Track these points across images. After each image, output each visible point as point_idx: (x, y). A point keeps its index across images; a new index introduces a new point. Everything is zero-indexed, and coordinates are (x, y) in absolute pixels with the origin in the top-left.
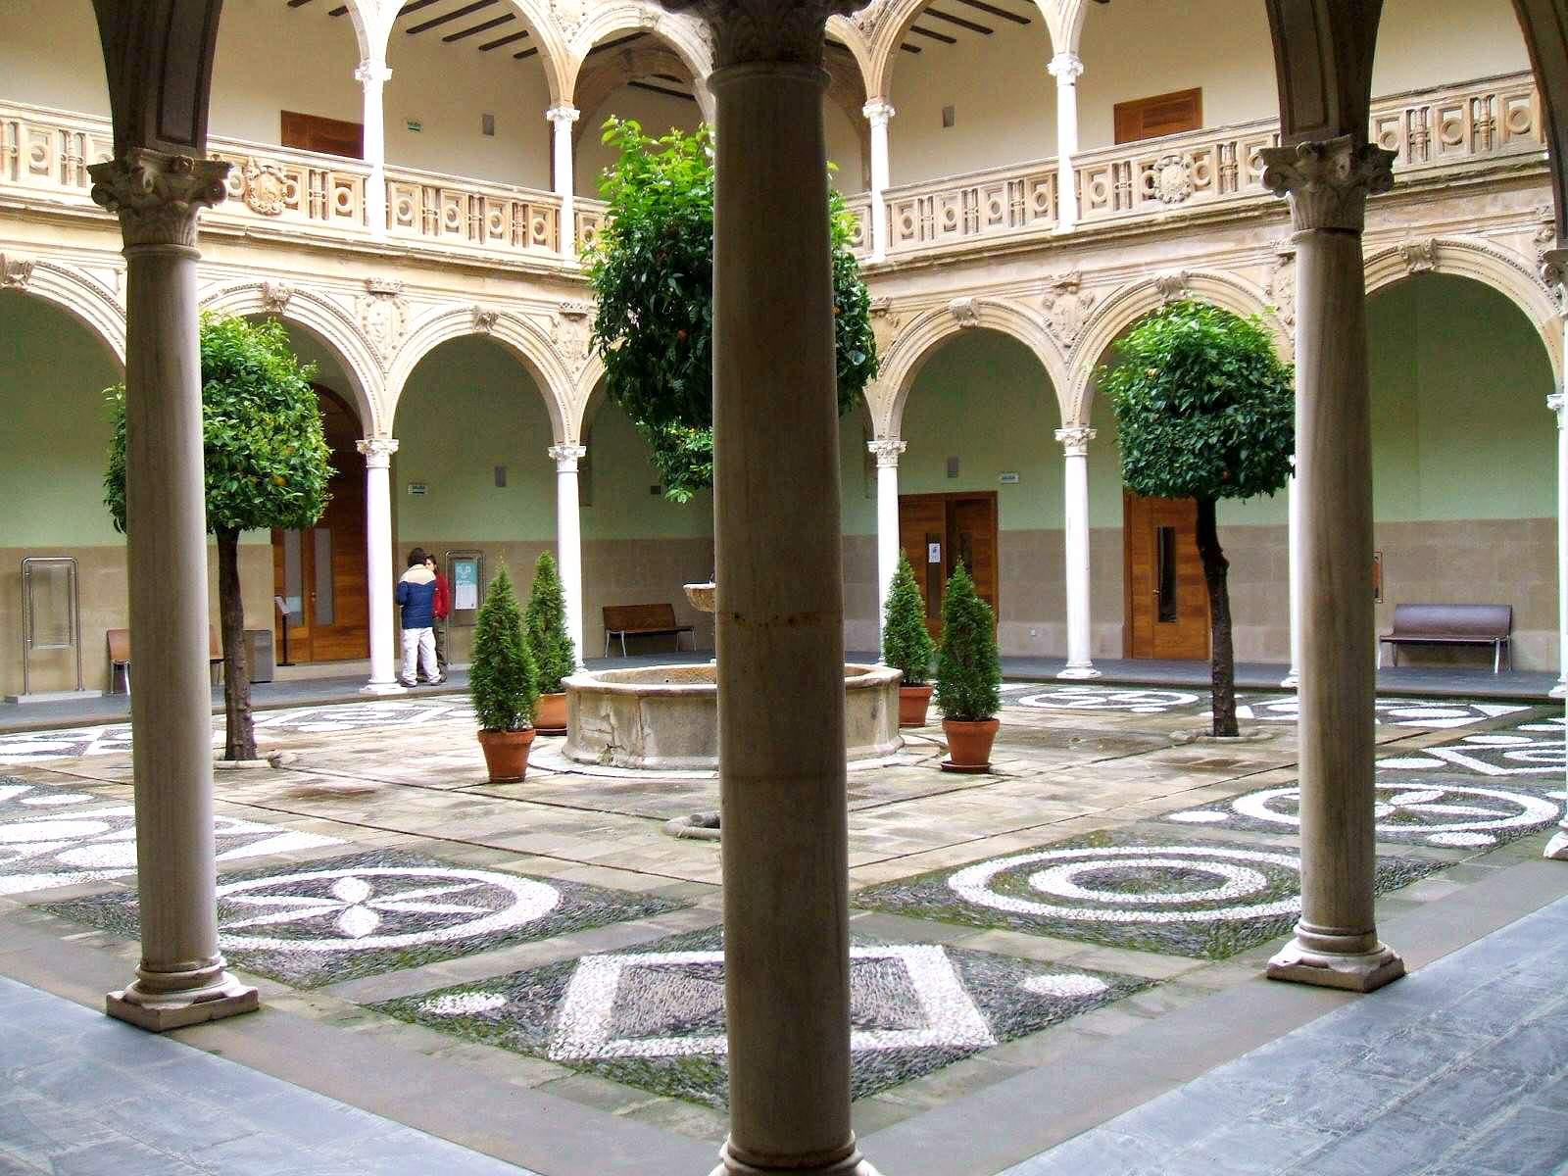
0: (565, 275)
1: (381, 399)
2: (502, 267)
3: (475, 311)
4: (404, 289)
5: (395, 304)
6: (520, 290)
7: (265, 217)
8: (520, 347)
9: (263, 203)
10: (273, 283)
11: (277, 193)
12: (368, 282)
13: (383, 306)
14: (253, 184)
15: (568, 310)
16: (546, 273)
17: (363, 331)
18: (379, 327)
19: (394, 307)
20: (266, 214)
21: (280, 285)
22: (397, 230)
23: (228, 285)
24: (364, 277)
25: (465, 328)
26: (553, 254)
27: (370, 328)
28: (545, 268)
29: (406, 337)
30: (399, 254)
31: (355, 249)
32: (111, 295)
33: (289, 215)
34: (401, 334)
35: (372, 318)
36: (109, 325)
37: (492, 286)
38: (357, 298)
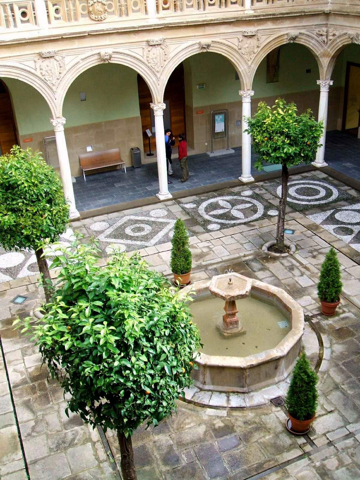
0: (244, 19)
1: (158, 87)
2: (212, 22)
3: (199, 43)
4: (166, 40)
5: (161, 48)
6: (223, 29)
7: (99, 22)
8: (223, 54)
9: (97, 17)
10: (103, 52)
11: (102, 10)
12: (148, 42)
13: (157, 51)
14: (91, 9)
15: (246, 34)
16: (235, 20)
17: (147, 63)
18: (154, 60)
19: (161, 50)
20: (98, 20)
21: (106, 53)
22: (162, 13)
23: (83, 56)
24: (145, 39)
25: (195, 51)
26: (241, 8)
27: (151, 61)
28: (234, 18)
29: (167, 61)
30: (161, 27)
31: (140, 29)
32: (33, 71)
33: (110, 18)
34: (165, 60)
35: (151, 55)
36: (35, 83)
37: (209, 30)
38: (143, 49)
